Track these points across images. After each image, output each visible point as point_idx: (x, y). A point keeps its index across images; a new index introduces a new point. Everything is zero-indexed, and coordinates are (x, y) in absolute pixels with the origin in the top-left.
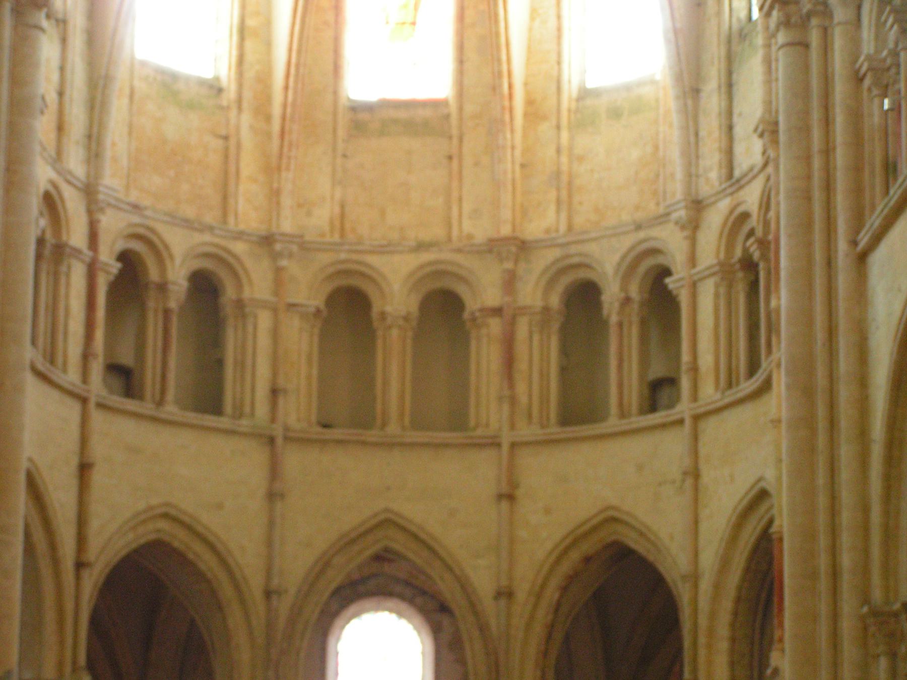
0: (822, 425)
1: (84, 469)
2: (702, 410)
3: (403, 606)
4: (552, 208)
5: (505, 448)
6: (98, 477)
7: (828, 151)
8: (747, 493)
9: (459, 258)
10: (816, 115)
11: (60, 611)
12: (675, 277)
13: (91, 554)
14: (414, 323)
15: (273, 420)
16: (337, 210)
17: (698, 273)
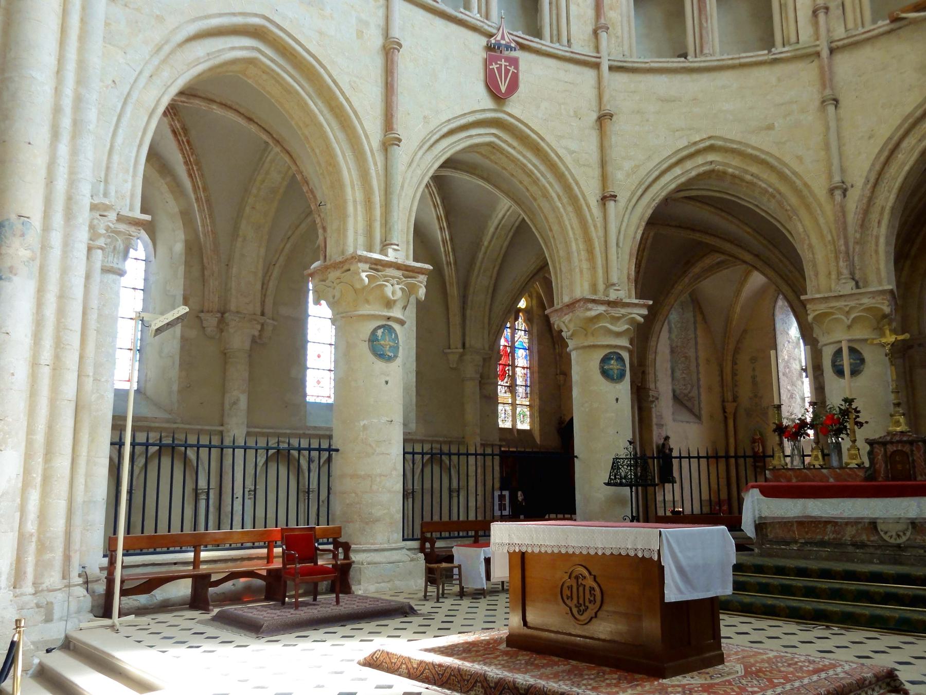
11: (588, 241)
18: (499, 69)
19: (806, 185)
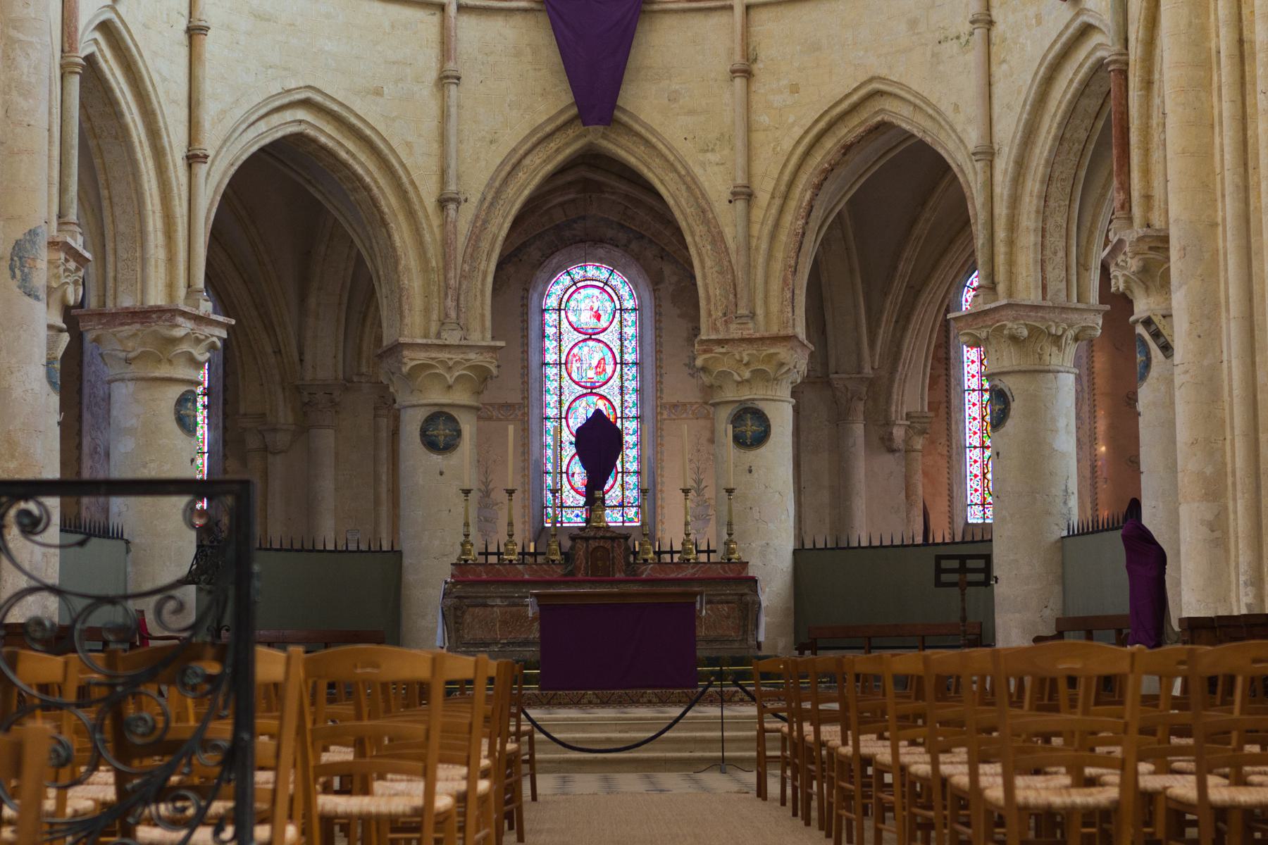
3: (617, 253)
5: (739, 11)
6: (211, 45)
13: (209, 143)
19: (412, 183)
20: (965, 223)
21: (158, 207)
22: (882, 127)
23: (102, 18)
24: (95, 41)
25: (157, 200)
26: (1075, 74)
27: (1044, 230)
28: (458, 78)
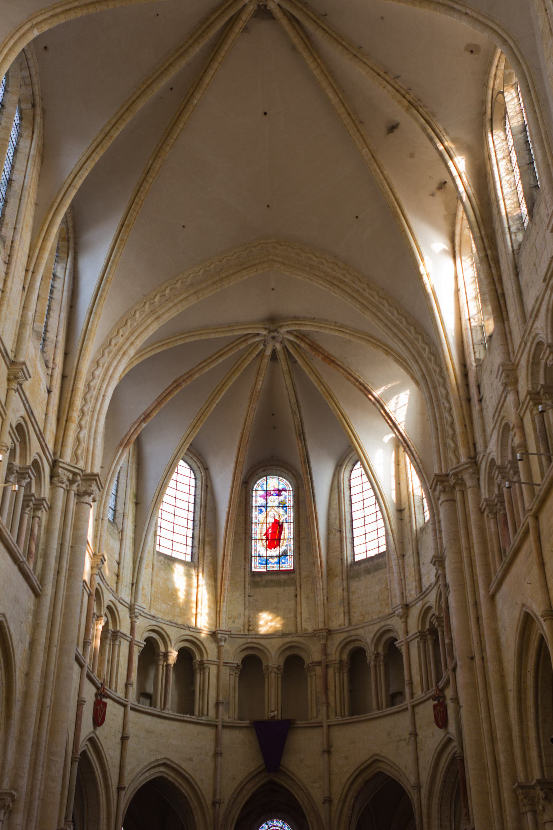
0: (480, 685)
1: (124, 739)
2: (416, 702)
4: (342, 615)
6: (130, 743)
7: (470, 548)
8: (441, 741)
9: (301, 640)
10: (462, 532)
12: (399, 641)
13: (126, 782)
14: (282, 671)
15: (217, 717)
16: (246, 620)
17: (410, 637)
18: (100, 709)
19: (203, 796)
20: (412, 815)
21: (105, 809)
22: (380, 774)
23: (89, 737)
24: (87, 745)
25: (105, 806)
26: (448, 756)
27: (441, 818)
28: (221, 754)
